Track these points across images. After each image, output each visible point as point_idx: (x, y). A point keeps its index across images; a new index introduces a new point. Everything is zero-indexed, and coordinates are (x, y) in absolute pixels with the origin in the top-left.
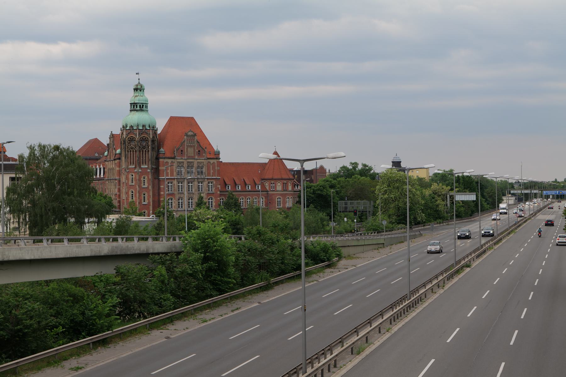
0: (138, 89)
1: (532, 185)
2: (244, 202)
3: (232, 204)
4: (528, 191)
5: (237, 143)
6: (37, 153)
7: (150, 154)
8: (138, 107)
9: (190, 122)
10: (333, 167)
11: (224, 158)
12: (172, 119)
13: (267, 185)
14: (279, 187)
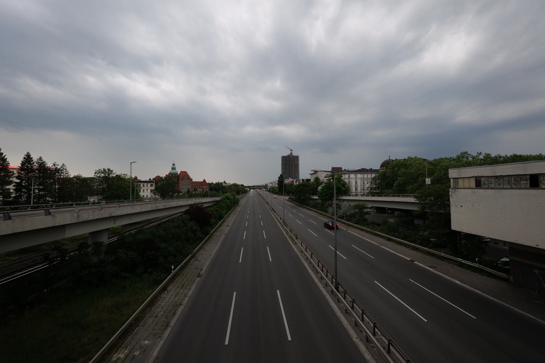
1: (254, 186)
2: (198, 190)
3: (195, 190)
4: (253, 187)
5: (196, 177)
7: (176, 180)
8: (173, 169)
9: (186, 172)
10: (214, 183)
11: (193, 181)
12: (182, 172)
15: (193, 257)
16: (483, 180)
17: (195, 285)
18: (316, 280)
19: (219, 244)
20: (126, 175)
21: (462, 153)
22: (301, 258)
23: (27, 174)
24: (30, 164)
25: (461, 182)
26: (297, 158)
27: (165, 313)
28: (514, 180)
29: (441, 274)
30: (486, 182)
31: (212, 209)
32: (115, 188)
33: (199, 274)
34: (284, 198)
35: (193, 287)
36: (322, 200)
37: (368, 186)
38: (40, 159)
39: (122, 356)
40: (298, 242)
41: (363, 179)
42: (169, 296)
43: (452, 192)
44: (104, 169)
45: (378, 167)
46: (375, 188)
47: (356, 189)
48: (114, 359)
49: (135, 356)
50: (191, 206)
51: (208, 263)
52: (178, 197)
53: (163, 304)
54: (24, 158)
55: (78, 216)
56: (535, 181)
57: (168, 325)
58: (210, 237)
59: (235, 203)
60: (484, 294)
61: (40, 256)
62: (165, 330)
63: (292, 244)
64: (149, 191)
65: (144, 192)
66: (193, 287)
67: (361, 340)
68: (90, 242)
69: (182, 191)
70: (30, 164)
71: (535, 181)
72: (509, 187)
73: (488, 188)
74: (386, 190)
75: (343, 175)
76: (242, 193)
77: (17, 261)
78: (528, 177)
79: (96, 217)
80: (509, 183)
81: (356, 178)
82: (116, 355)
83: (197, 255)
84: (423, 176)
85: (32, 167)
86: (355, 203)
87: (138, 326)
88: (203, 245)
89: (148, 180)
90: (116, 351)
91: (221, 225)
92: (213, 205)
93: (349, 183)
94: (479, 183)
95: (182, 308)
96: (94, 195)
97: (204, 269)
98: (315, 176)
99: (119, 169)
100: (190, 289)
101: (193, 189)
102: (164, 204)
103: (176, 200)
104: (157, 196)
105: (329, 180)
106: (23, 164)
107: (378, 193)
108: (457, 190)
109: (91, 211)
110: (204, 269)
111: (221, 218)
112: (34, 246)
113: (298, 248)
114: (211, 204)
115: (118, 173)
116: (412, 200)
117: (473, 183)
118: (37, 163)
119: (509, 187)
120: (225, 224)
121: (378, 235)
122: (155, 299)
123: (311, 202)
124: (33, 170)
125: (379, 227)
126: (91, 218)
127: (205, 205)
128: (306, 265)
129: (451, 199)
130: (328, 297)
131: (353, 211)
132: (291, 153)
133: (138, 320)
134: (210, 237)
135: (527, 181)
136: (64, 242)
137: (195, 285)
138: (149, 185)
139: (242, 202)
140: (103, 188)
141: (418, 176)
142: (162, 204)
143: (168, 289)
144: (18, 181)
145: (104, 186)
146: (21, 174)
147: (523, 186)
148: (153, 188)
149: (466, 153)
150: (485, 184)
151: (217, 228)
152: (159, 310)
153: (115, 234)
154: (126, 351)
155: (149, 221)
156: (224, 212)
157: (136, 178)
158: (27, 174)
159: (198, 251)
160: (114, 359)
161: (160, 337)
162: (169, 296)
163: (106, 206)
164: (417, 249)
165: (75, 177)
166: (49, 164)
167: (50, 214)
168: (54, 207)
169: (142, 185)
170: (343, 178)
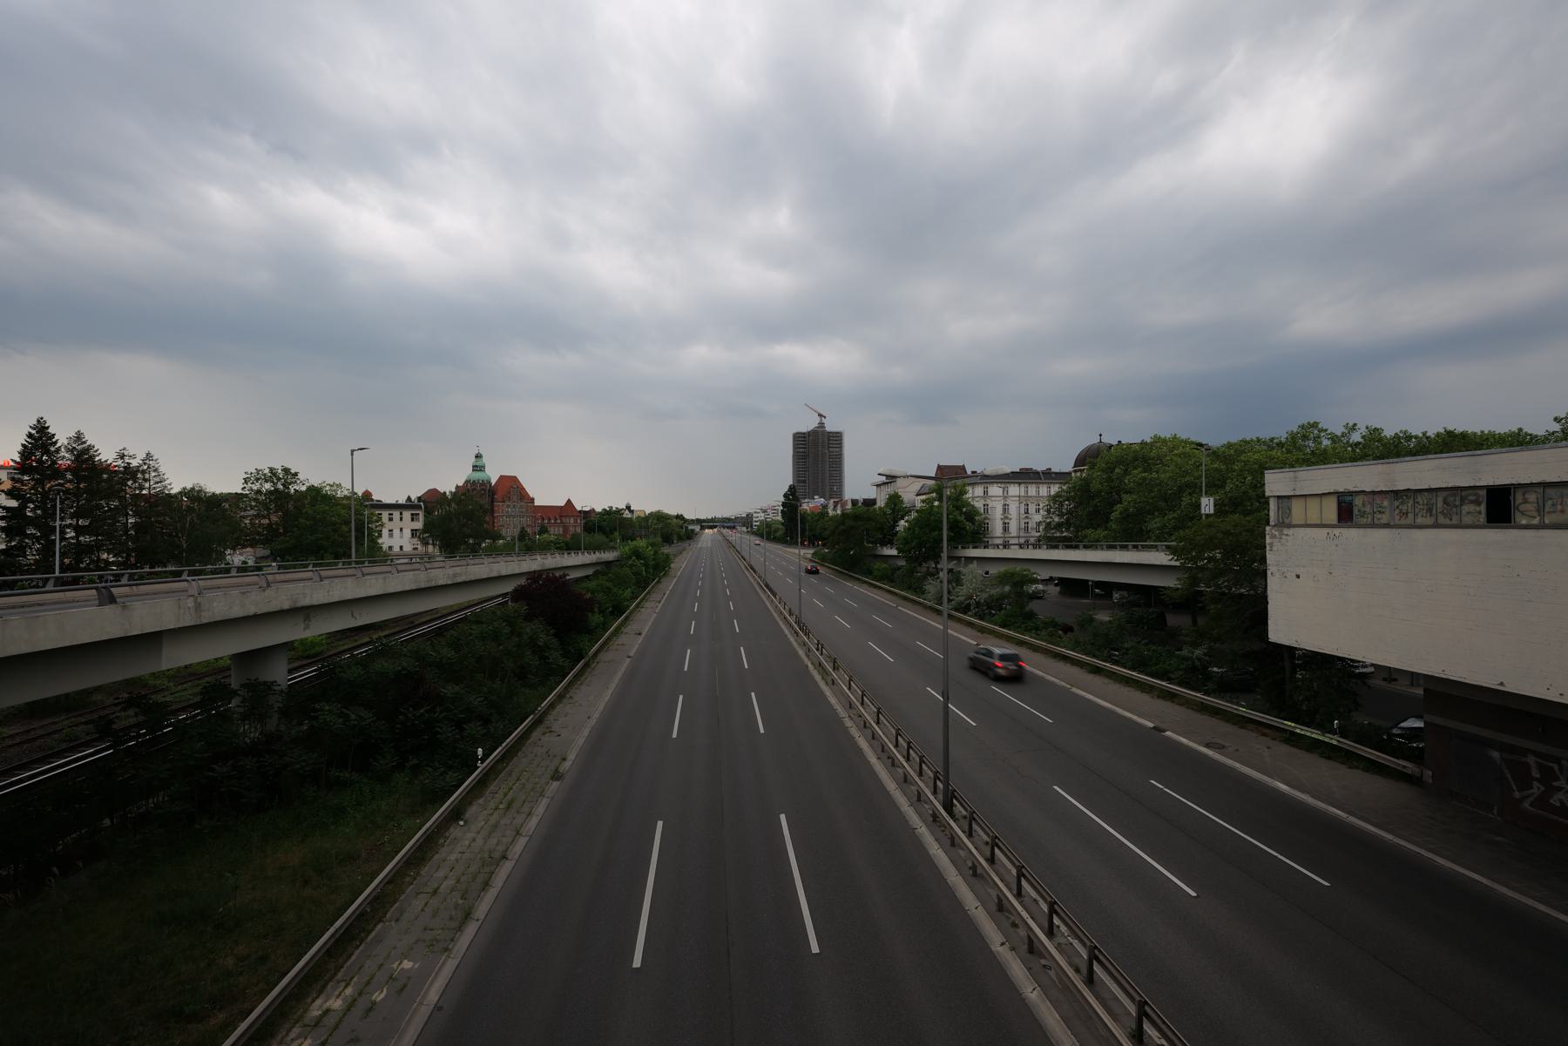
1: (713, 520)
2: (552, 530)
3: (543, 530)
4: (710, 523)
5: (545, 494)
7: (485, 501)
8: (476, 468)
9: (514, 479)
10: (599, 509)
12: (502, 478)
15: (538, 722)
16: (1358, 501)
17: (544, 803)
18: (891, 786)
19: (613, 686)
20: (339, 486)
21: (1302, 427)
22: (848, 723)
23: (40, 482)
24: (47, 452)
25: (1297, 508)
26: (836, 438)
27: (458, 881)
28: (1445, 502)
29: (1237, 765)
30: (1368, 509)
31: (593, 584)
32: (306, 525)
33: (557, 770)
34: (801, 555)
35: (541, 809)
36: (909, 559)
37: (1038, 518)
38: (79, 437)
39: (336, 1004)
40: (841, 678)
41: (1024, 500)
42: (470, 835)
43: (1274, 536)
44: (271, 469)
45: (1066, 465)
46: (1059, 526)
47: (1006, 529)
48: (315, 1012)
49: (374, 1003)
50: (534, 576)
51: (581, 741)
52: (494, 552)
53: (453, 857)
54: (30, 435)
55: (198, 607)
56: (1499, 506)
57: (468, 916)
58: (587, 665)
59: (660, 568)
60: (1352, 819)
61: (86, 723)
62: (460, 929)
63: (822, 685)
64: (407, 533)
66: (541, 809)
67: (1013, 949)
68: (234, 683)
69: (503, 532)
70: (47, 452)
71: (1499, 506)
72: (1430, 521)
73: (1373, 526)
74: (1089, 531)
75: (969, 488)
76: (680, 539)
77: (18, 740)
78: (1483, 493)
79: (252, 610)
80: (1430, 510)
81: (1005, 498)
82: (319, 1002)
83: (551, 717)
84: (1194, 489)
85: (54, 462)
86: (1002, 568)
87: (380, 921)
88: (566, 689)
89: (402, 500)
90: (320, 992)
91: (617, 631)
92: (596, 573)
93: (986, 510)
94: (1347, 510)
95: (507, 866)
96: (244, 547)
97: (571, 757)
98: (890, 490)
99: (319, 469)
100: (530, 814)
101: (537, 529)
102: (451, 571)
103: (486, 560)
104: (430, 548)
105: (929, 502)
106: (26, 453)
107: (1065, 539)
108: (1286, 531)
109: (235, 592)
110: (571, 757)
111: (618, 610)
112: (67, 695)
113: (840, 694)
114: (590, 572)
115: (315, 481)
116: (1160, 558)
117: (1331, 511)
118: (72, 451)
119: (1430, 521)
120: (631, 628)
121: (1065, 658)
122: (430, 844)
123: (878, 565)
124: (57, 473)
125: (1069, 634)
126: (237, 612)
127: (573, 575)
128: (863, 744)
129: (1269, 556)
130: (923, 831)
131: (995, 591)
132: (822, 425)
133: (380, 903)
134: (587, 665)
135: (1479, 504)
136: (158, 682)
137: (544, 803)
138: (407, 514)
139: (680, 565)
140: (270, 525)
141: (1181, 490)
142: (446, 571)
143: (467, 815)
144: (14, 504)
145: (274, 518)
146: (22, 482)
147: (1467, 520)
148: (419, 525)
149: (1315, 425)
150: (1363, 514)
151: (609, 639)
152: (441, 874)
153: (308, 657)
154: (349, 991)
155: (408, 622)
156: (628, 593)
157: (367, 495)
158: (40, 482)
159: (552, 706)
160: (315, 1012)
161: (446, 950)
162: (470, 835)
163: (279, 577)
164: (1170, 696)
165: (184, 492)
166: (106, 454)
167: (112, 600)
168: (124, 580)
169: (385, 515)
170: (969, 495)
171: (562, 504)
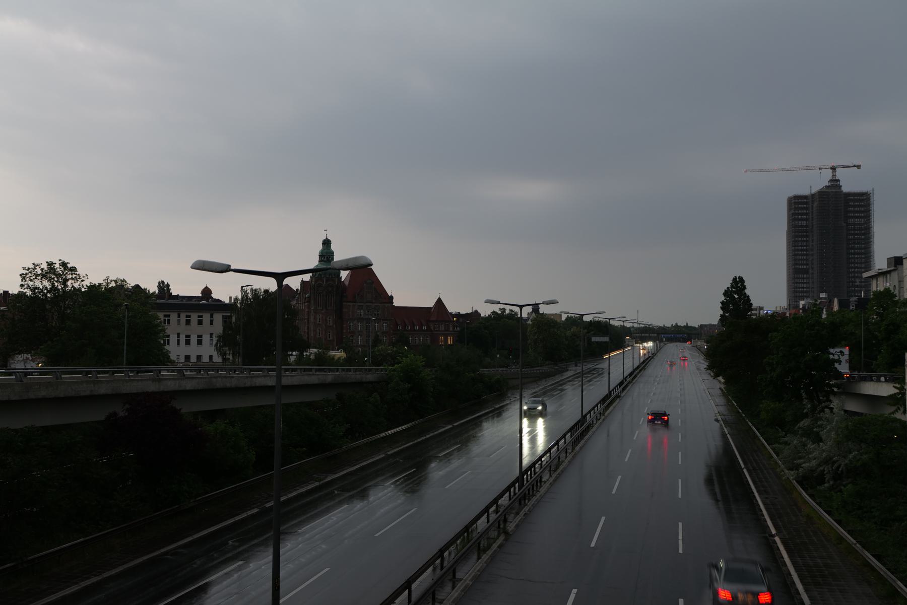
0: (327, 243)
6: (250, 296)
11: (397, 303)
13: (432, 326)
14: (442, 328)
44: (50, 264)
65: (200, 342)
132: (835, 183)
138: (218, 318)
157: (207, 292)
171: (430, 303)
